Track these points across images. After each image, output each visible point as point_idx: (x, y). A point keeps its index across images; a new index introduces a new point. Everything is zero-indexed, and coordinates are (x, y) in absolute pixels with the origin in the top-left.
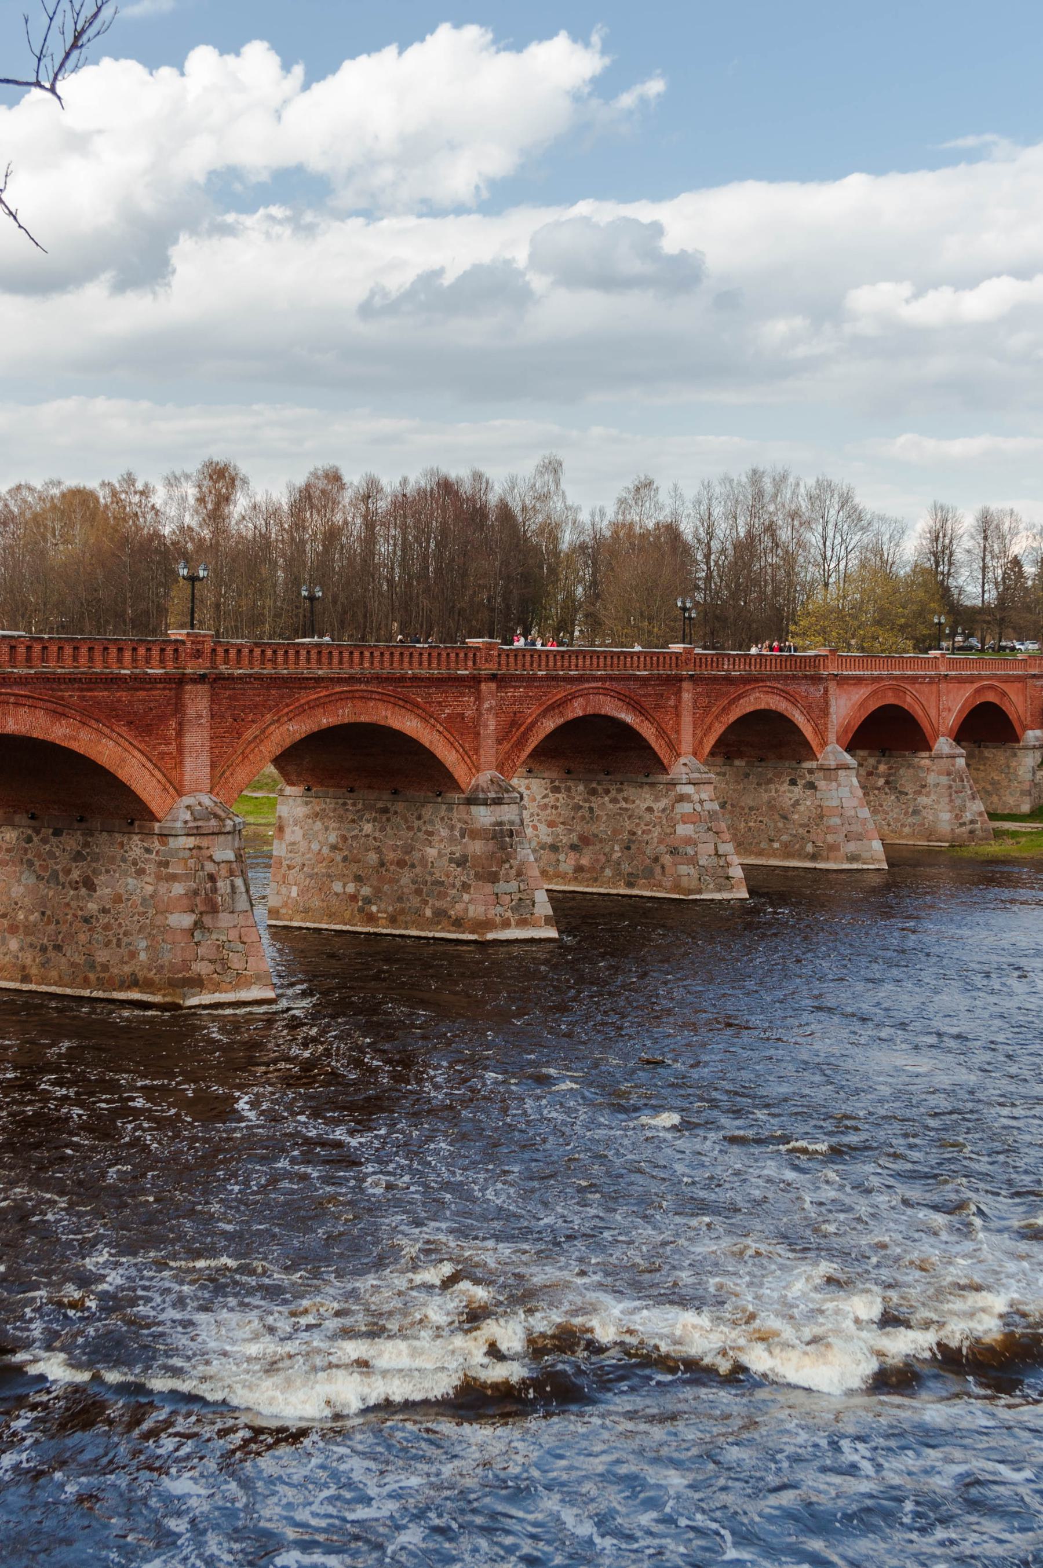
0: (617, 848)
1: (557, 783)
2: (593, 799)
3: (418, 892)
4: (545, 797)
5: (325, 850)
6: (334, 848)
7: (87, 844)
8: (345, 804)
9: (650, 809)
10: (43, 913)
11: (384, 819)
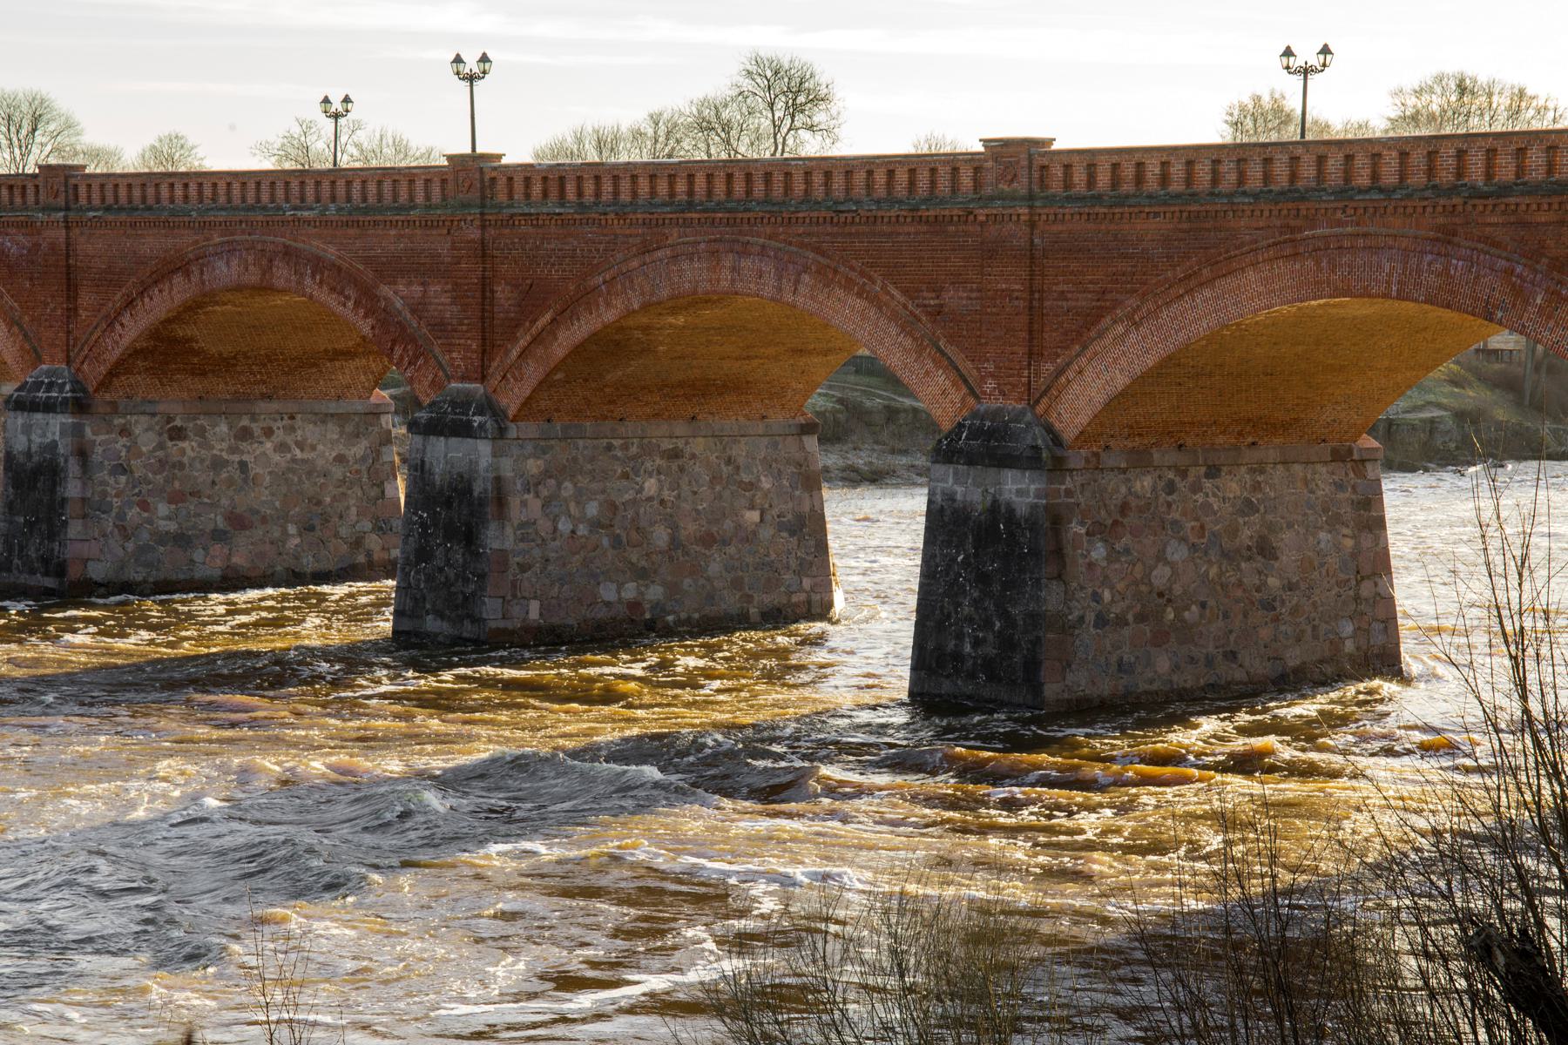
0: (292, 529)
1: (178, 423)
2: (244, 445)
3: (737, 584)
4: (161, 446)
5: (582, 530)
6: (595, 525)
7: (1257, 487)
8: (609, 448)
9: (340, 459)
10: (1203, 605)
11: (674, 467)
